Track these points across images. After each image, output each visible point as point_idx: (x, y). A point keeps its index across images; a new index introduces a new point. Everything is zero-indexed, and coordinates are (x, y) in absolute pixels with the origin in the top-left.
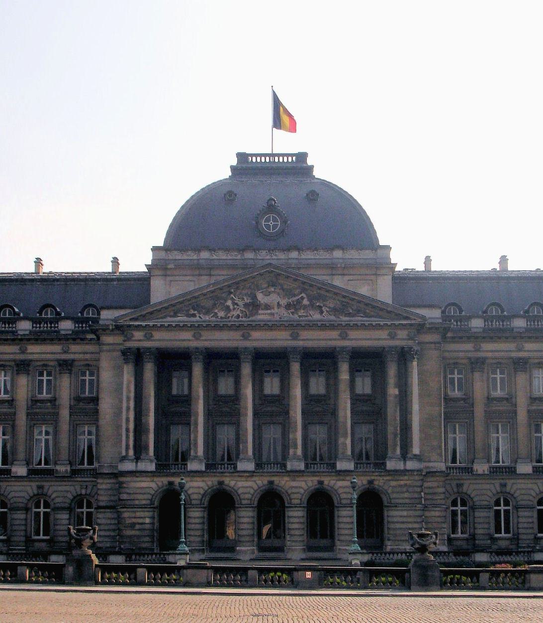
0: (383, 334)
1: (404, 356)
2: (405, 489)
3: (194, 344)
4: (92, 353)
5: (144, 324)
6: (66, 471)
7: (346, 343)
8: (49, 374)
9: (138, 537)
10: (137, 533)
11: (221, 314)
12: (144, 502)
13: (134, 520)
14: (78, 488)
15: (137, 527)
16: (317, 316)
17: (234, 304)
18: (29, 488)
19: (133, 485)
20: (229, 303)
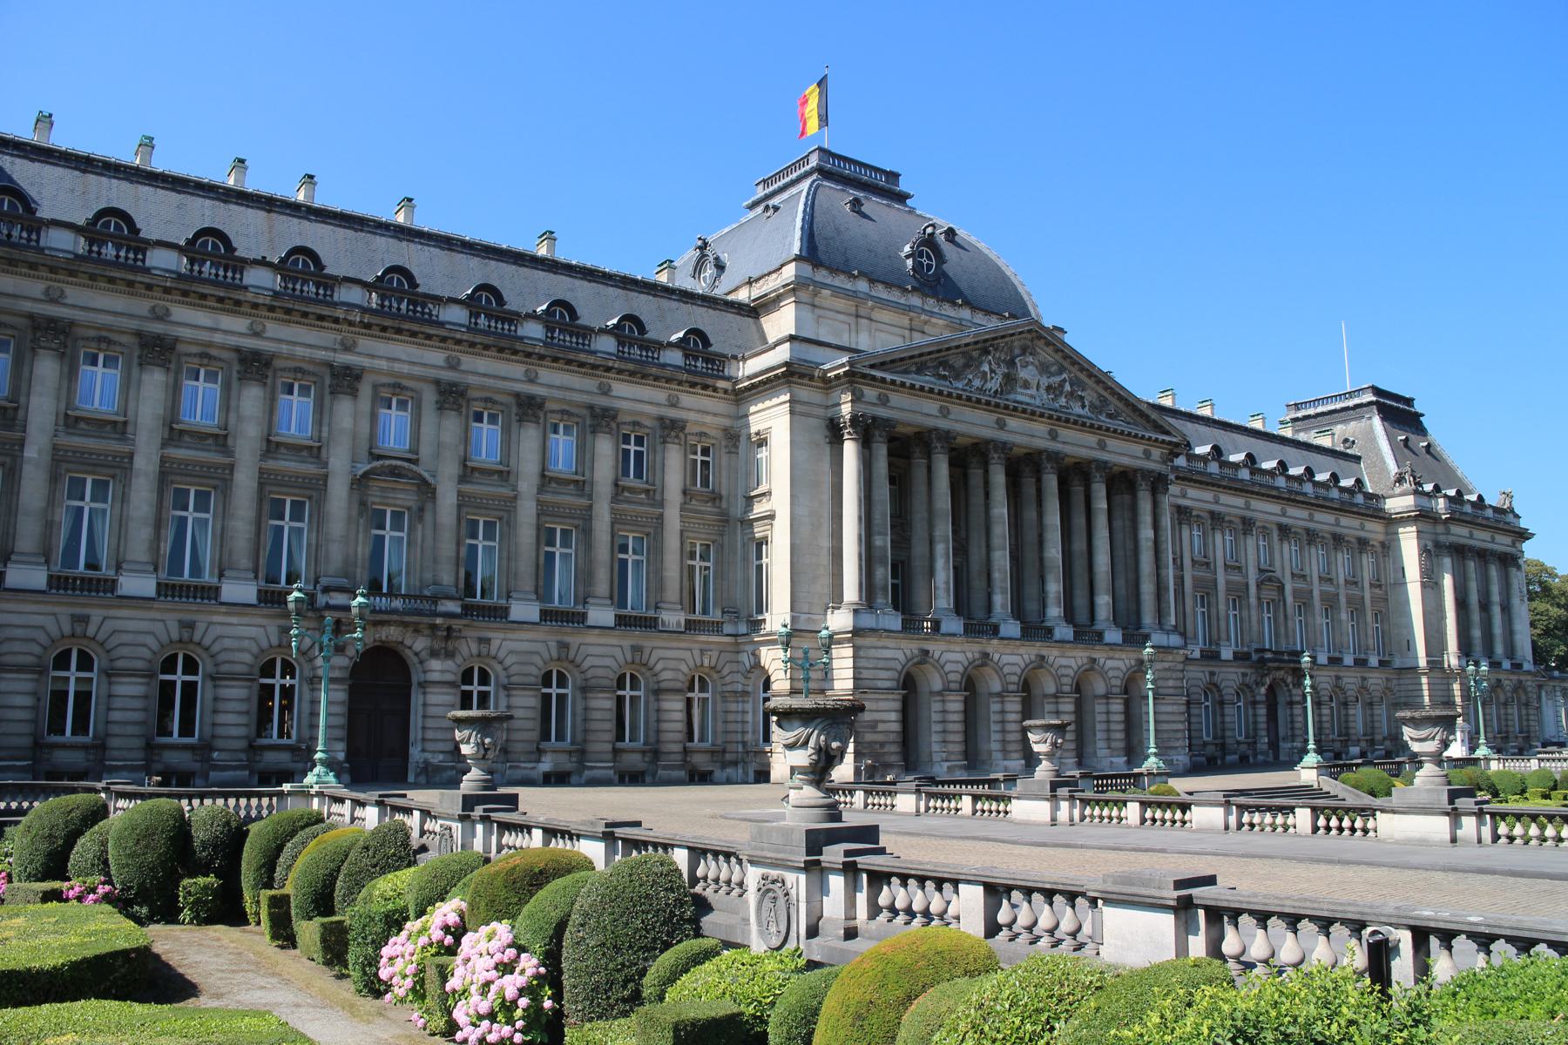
0: (1138, 449)
1: (1158, 483)
2: (1169, 674)
3: (943, 424)
4: (715, 415)
5: (889, 377)
6: (678, 624)
7: (1105, 456)
8: (639, 441)
9: (882, 744)
10: (880, 738)
11: (977, 383)
12: (888, 684)
13: (876, 716)
14: (697, 653)
15: (881, 727)
16: (1077, 409)
17: (992, 371)
18: (618, 652)
19: (873, 653)
20: (986, 368)
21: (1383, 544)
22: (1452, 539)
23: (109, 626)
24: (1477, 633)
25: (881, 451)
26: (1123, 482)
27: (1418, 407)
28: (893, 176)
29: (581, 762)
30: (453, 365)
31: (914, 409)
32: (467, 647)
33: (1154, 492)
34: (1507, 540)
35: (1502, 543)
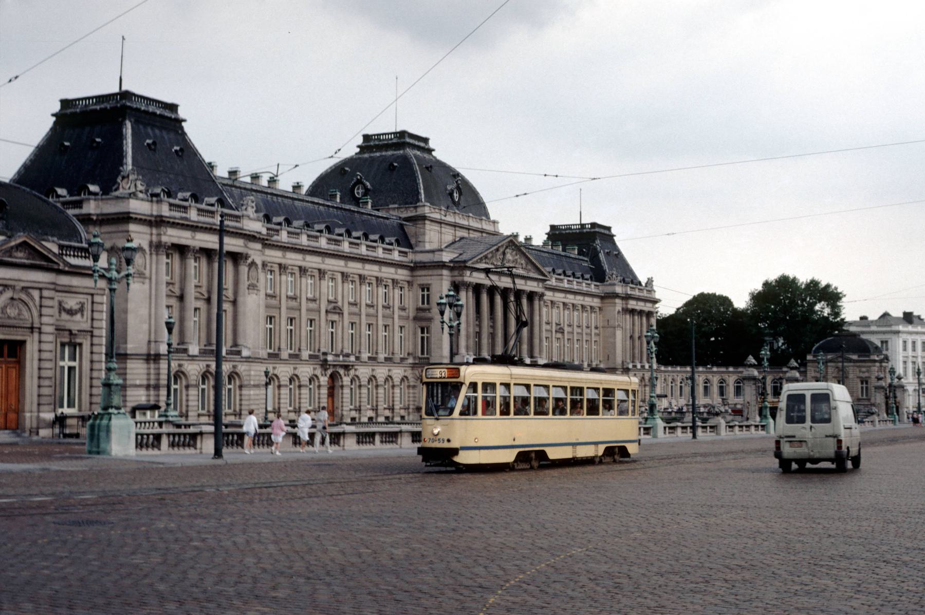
0: (535, 284)
21: (600, 309)
22: (630, 307)
23: (280, 369)
24: (637, 351)
25: (470, 294)
26: (531, 296)
27: (613, 231)
28: (426, 140)
29: (377, 413)
30: (346, 266)
31: (479, 278)
32: (352, 372)
33: (540, 300)
34: (649, 305)
35: (647, 307)
